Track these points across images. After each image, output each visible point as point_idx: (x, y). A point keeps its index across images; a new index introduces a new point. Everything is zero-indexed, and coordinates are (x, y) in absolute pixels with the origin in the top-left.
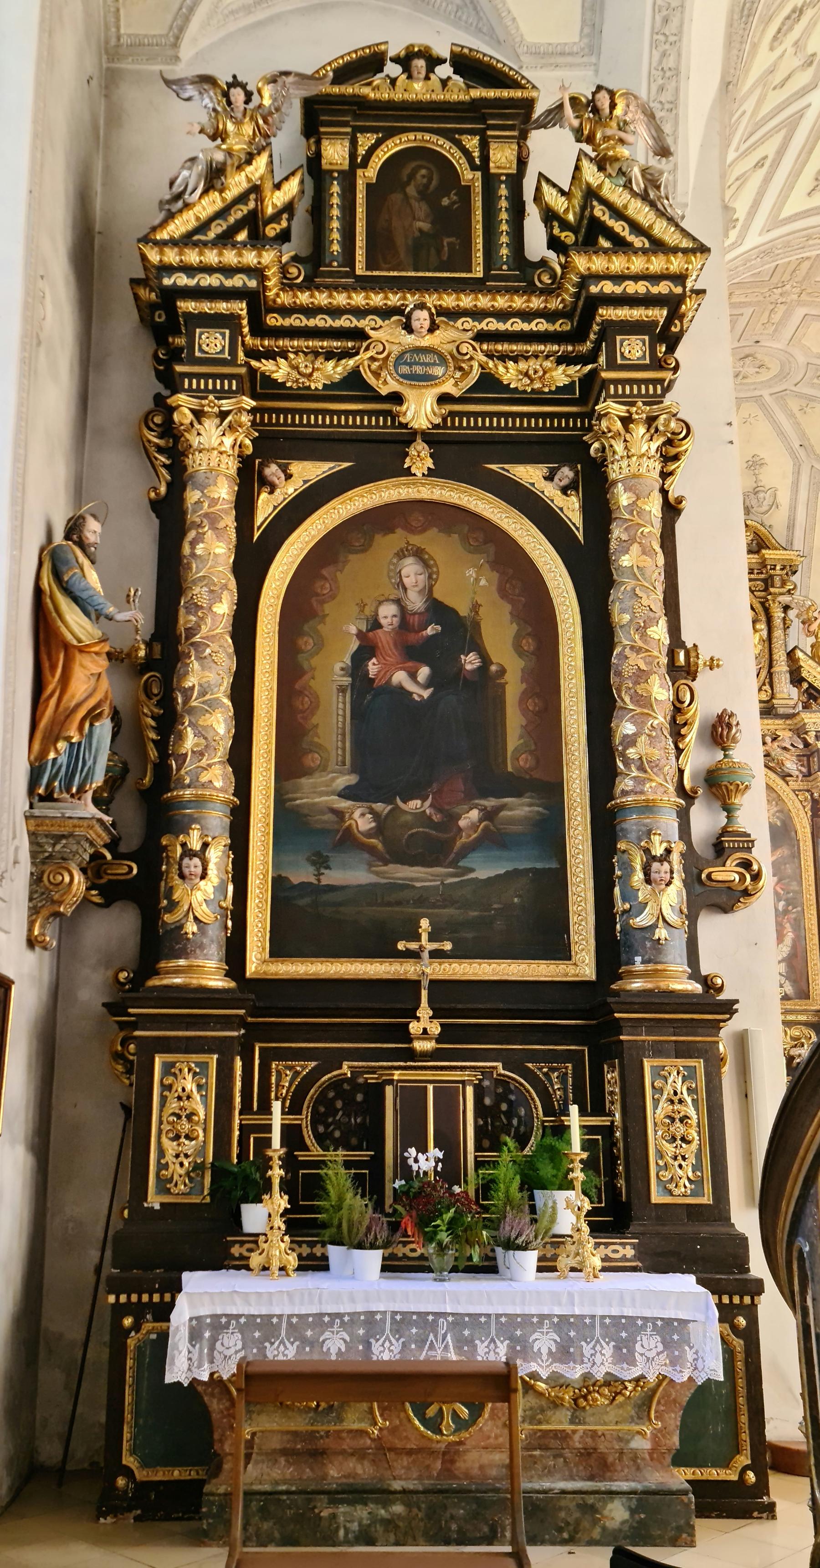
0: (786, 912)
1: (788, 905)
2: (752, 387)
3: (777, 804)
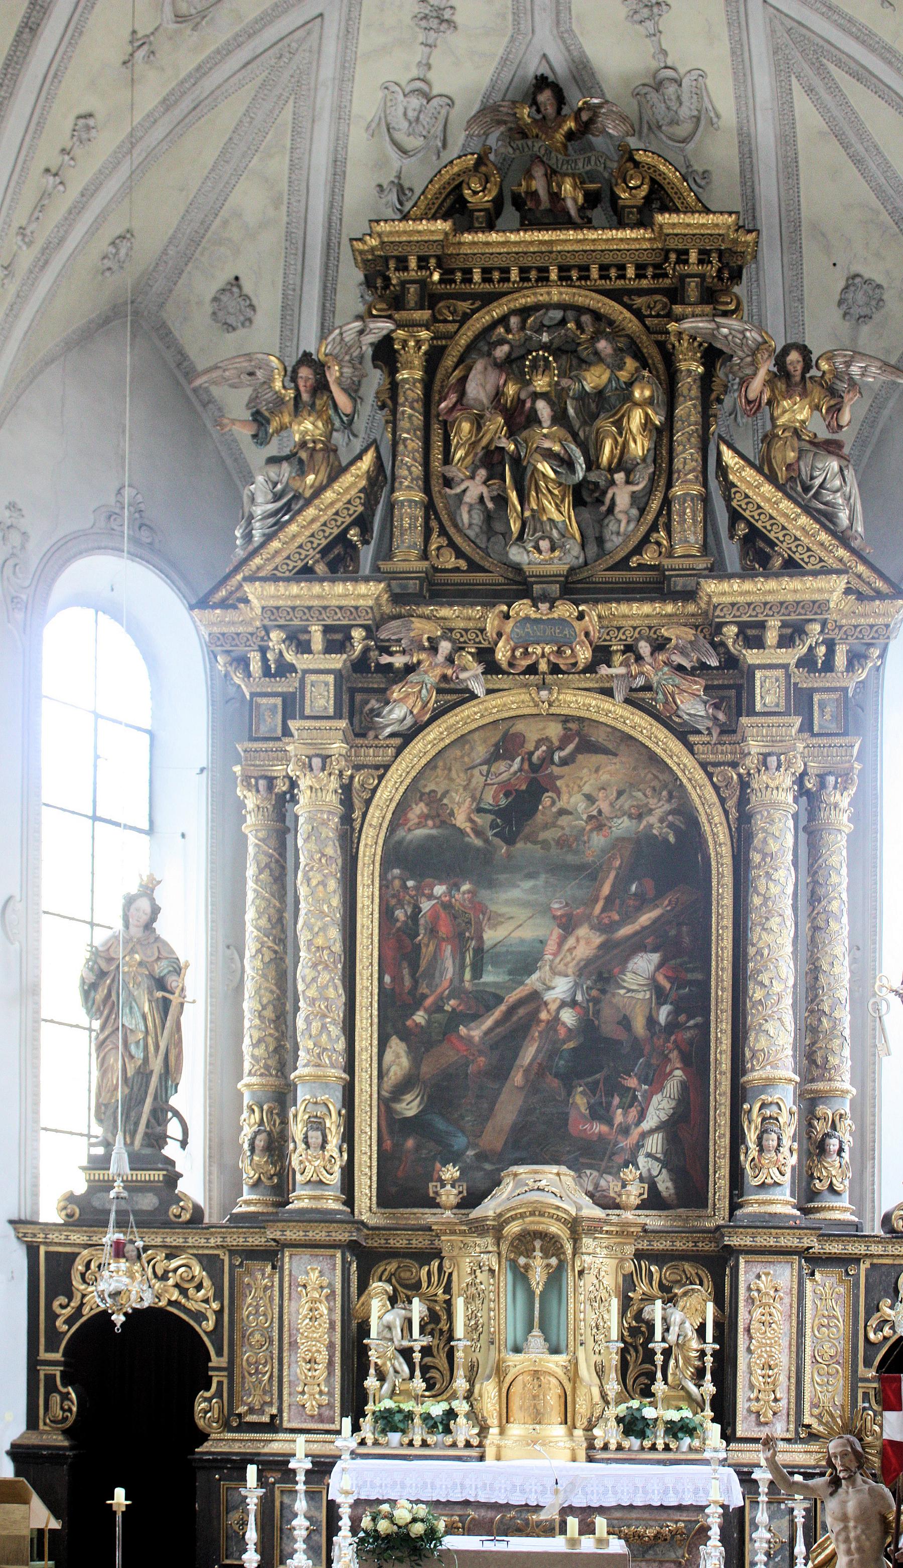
0: (672, 1026)
1: (676, 1012)
3: (671, 797)
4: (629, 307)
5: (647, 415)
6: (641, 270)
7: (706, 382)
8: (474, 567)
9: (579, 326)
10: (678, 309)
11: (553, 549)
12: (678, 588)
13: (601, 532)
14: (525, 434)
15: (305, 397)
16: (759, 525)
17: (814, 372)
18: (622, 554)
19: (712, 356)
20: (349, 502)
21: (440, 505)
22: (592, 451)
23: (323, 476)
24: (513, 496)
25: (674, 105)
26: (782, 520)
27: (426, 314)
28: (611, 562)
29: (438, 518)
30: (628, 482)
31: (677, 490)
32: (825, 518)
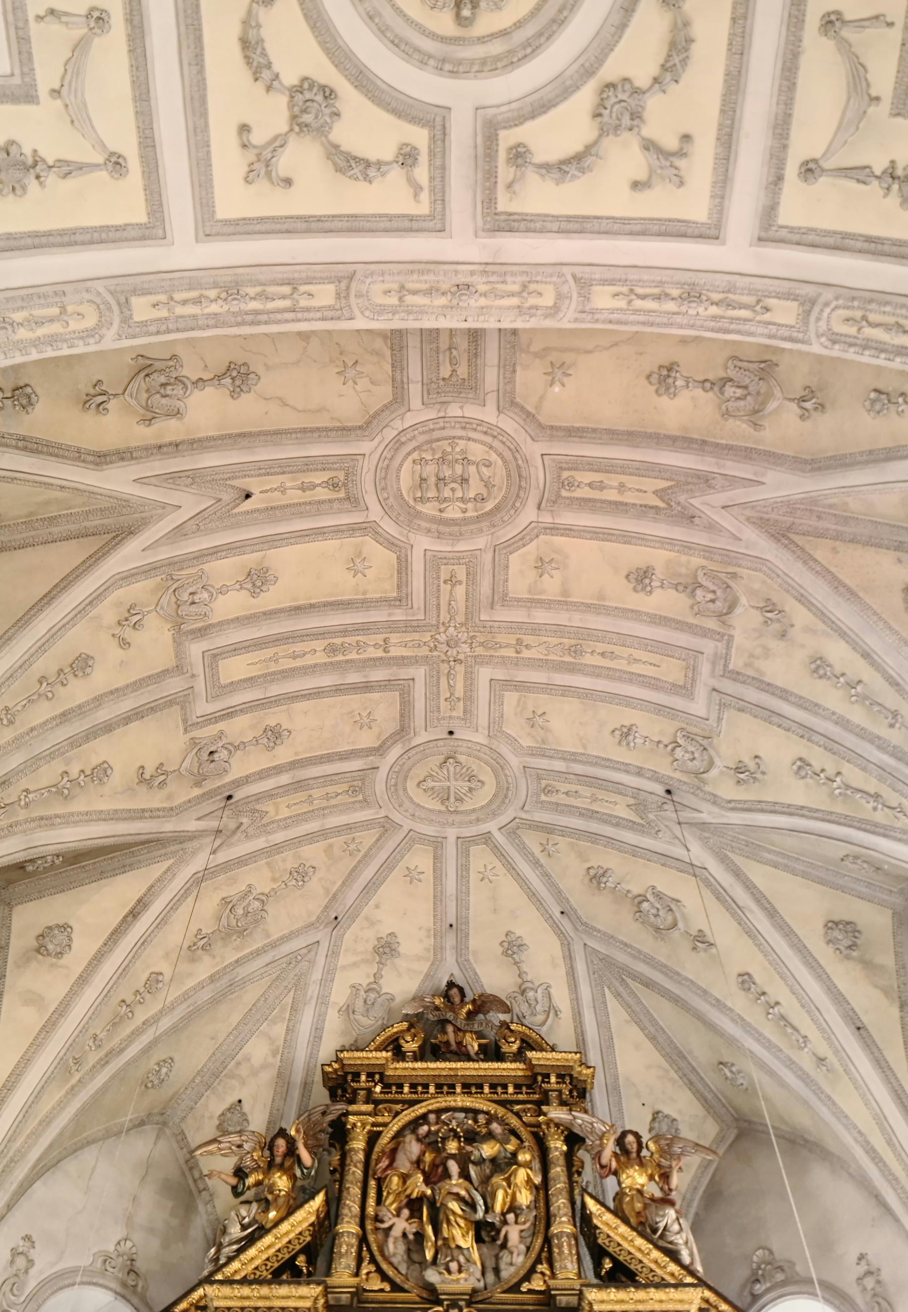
2: (473, 817)
4: (512, 1111)
5: (528, 1175)
6: (517, 1087)
7: (569, 1157)
8: (396, 1287)
9: (476, 1121)
10: (544, 1108)
11: (460, 1271)
12: (563, 1305)
13: (497, 1264)
14: (439, 1185)
15: (278, 1160)
16: (621, 1258)
17: (644, 1153)
18: (515, 1280)
19: (574, 1140)
20: (300, 1233)
21: (371, 1238)
22: (489, 1200)
23: (283, 1212)
24: (429, 1230)
25: (533, 1003)
26: (639, 1255)
27: (369, 1107)
28: (506, 1287)
29: (369, 1250)
30: (516, 1222)
31: (554, 1230)
32: (673, 1255)
